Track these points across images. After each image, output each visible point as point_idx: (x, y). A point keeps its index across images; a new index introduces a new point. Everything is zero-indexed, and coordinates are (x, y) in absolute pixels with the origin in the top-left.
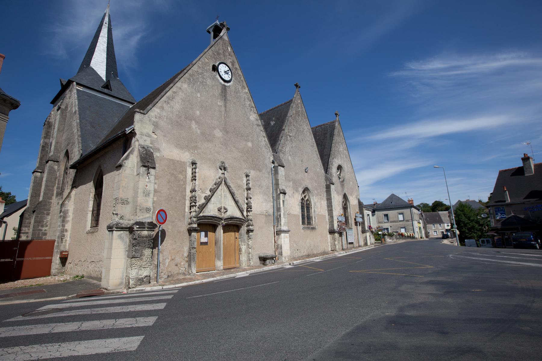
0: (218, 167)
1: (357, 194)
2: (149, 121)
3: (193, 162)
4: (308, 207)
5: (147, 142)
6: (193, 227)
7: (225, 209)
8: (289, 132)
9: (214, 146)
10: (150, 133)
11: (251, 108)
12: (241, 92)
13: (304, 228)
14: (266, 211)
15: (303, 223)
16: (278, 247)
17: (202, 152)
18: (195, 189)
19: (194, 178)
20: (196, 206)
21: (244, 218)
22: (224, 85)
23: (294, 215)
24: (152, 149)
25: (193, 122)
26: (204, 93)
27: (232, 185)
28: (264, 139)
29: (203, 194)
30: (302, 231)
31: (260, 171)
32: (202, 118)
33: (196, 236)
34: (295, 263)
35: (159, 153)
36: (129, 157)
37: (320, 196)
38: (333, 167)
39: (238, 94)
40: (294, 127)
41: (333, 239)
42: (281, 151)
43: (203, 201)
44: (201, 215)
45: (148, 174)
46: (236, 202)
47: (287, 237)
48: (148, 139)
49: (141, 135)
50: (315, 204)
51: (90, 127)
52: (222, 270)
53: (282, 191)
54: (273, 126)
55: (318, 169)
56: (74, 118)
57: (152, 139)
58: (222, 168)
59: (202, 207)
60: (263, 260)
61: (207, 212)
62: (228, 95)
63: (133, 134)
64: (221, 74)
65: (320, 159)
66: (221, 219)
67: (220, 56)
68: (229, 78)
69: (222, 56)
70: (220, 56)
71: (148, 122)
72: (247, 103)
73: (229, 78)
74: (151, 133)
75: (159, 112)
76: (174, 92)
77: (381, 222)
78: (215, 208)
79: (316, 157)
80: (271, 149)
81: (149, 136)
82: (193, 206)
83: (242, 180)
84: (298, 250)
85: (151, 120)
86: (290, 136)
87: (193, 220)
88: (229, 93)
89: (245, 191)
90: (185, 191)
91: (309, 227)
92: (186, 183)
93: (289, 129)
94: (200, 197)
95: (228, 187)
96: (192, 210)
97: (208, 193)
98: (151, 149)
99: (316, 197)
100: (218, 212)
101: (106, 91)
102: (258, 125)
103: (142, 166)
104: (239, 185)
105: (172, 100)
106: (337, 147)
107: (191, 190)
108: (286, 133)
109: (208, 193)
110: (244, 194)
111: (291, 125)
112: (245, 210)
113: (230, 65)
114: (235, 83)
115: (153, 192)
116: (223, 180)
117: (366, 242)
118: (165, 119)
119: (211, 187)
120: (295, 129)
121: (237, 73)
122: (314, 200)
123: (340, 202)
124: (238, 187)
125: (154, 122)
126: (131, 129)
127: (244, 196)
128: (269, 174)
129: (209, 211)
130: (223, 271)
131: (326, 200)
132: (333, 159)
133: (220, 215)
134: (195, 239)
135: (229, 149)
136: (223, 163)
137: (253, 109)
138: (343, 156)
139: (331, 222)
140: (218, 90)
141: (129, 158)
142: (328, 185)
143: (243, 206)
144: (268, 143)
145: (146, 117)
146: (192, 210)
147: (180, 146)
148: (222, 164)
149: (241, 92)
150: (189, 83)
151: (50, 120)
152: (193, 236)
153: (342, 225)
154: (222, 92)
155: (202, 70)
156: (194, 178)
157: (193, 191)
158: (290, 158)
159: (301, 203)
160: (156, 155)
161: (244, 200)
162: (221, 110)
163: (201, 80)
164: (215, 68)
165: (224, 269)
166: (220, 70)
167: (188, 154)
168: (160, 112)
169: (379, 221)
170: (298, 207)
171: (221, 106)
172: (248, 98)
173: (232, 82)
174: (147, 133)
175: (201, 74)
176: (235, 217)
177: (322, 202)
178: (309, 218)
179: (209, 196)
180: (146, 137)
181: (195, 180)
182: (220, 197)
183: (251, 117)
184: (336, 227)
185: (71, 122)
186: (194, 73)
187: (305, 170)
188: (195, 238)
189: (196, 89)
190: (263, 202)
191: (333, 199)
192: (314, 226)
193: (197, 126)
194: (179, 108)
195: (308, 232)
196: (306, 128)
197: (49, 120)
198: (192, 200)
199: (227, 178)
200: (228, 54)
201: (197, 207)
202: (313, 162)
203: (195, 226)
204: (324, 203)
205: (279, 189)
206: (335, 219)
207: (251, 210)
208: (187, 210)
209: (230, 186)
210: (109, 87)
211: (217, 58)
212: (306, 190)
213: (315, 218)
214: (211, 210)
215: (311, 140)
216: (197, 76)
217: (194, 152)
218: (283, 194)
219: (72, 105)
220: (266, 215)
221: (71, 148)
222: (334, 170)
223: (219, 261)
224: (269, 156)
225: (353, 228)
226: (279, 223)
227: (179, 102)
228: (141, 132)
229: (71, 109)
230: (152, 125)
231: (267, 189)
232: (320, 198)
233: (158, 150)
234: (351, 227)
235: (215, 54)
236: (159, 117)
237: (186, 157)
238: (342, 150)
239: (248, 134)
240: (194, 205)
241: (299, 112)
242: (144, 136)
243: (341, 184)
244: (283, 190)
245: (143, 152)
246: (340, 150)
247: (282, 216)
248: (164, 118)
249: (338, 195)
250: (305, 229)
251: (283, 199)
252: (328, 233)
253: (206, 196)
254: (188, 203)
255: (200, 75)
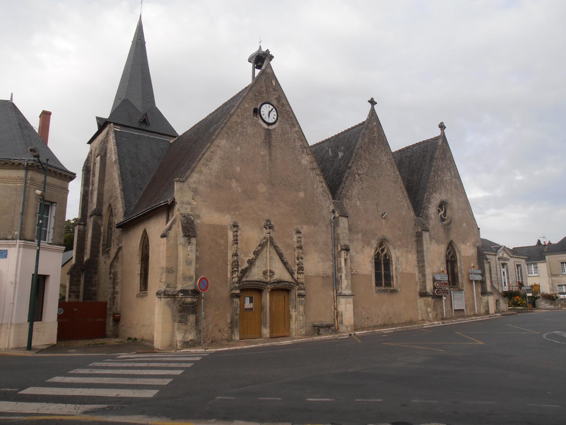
0: (263, 226)
1: (476, 240)
2: (189, 189)
3: (235, 224)
4: (388, 263)
5: (187, 210)
6: (236, 293)
7: (271, 272)
8: (357, 169)
9: (258, 203)
10: (189, 201)
11: (303, 149)
12: (289, 132)
13: (378, 292)
14: (323, 272)
15: (378, 284)
16: (337, 314)
17: (244, 212)
18: (237, 253)
19: (236, 241)
20: (238, 271)
21: (294, 282)
22: (268, 129)
23: (363, 275)
24: (192, 216)
25: (234, 181)
26: (245, 145)
27: (279, 245)
28: (320, 185)
29: (246, 258)
30: (376, 295)
31: (315, 224)
32: (242, 175)
33: (239, 302)
34: (358, 334)
35: (200, 219)
36: (172, 227)
37: (405, 249)
38: (429, 206)
39: (286, 136)
40: (366, 161)
41: (424, 305)
42: (345, 196)
43: (246, 265)
44: (244, 279)
45: (189, 243)
46: (285, 264)
47: (349, 303)
48: (189, 207)
49: (182, 204)
50: (397, 259)
51: (130, 177)
52: (268, 338)
53: (344, 248)
54: (341, 160)
55: (404, 212)
56: (115, 168)
57: (192, 206)
58: (267, 227)
59: (244, 272)
60: (317, 329)
61: (251, 277)
62: (273, 141)
63: (173, 203)
64: (264, 118)
65: (407, 198)
66: (267, 283)
67: (262, 96)
68: (274, 119)
69: (265, 94)
70: (262, 96)
71: (187, 190)
72: (297, 144)
73: (274, 119)
74: (190, 200)
75: (197, 176)
76: (212, 152)
77: (557, 275)
78: (260, 272)
79: (401, 196)
80: (330, 196)
81: (189, 203)
82: (235, 271)
83: (292, 238)
84: (368, 318)
85: (190, 187)
86: (359, 175)
87: (236, 286)
88: (275, 138)
89: (295, 251)
90: (227, 256)
91: (387, 290)
92: (228, 247)
93: (357, 165)
94: (243, 261)
95: (276, 247)
96: (234, 276)
97: (252, 256)
98: (192, 217)
99: (399, 250)
100: (263, 276)
101: (144, 127)
102: (313, 169)
103: (184, 236)
104: (288, 244)
105: (209, 161)
106: (440, 176)
107: (233, 254)
108: (353, 171)
109: (252, 256)
110: (295, 254)
111: (362, 159)
112: (296, 273)
113: (275, 103)
114: (281, 123)
115: (194, 260)
116: (269, 240)
117: (487, 309)
118: (204, 183)
119: (254, 249)
120: (367, 163)
121: (285, 110)
122: (396, 254)
123: (441, 253)
124: (287, 246)
125: (193, 188)
126: (172, 199)
127: (295, 256)
128: (327, 228)
129: (254, 276)
130: (270, 339)
131: (416, 252)
132: (431, 194)
133: (265, 279)
134: (238, 305)
135: (275, 204)
136: (268, 221)
137: (307, 150)
138: (451, 187)
139: (422, 282)
140: (261, 138)
141: (172, 228)
142: (420, 231)
143: (293, 268)
144: (326, 188)
145: (185, 185)
146: (234, 276)
147: (219, 209)
148: (267, 222)
149: (289, 132)
150: (228, 137)
151: (89, 164)
152: (236, 302)
153: (442, 286)
154: (266, 139)
155: (242, 119)
156: (236, 241)
157: (236, 255)
158: (358, 203)
159: (374, 260)
160: (198, 221)
161: (295, 261)
162: (265, 160)
163: (241, 131)
164: (257, 112)
165: (270, 337)
166: (262, 113)
167: (229, 216)
168: (199, 177)
169: (552, 274)
170: (370, 264)
171: (265, 155)
172: (299, 137)
173: (277, 123)
174: (187, 201)
175: (240, 124)
176: (283, 281)
177: (410, 256)
178: (388, 277)
179: (253, 259)
180: (186, 205)
181: (237, 243)
182: (265, 259)
183: (303, 160)
184: (429, 287)
185: (111, 172)
186: (232, 125)
187: (382, 216)
188: (238, 304)
189: (235, 142)
190: (319, 262)
191: (427, 251)
192: (395, 287)
193: (237, 185)
194: (218, 168)
195: (385, 296)
196: (385, 158)
197: (88, 164)
198: (234, 266)
199: (274, 238)
200: (272, 90)
201: (239, 272)
202: (395, 204)
203: (238, 291)
204: (413, 257)
205: (340, 246)
206: (429, 279)
207: (302, 272)
208: (229, 275)
209: (277, 246)
210: (146, 121)
211: (258, 98)
212: (382, 243)
213: (397, 277)
214: (255, 275)
215: (392, 174)
216: (237, 127)
217: (235, 214)
218: (345, 251)
219: (111, 151)
220: (323, 277)
221: (114, 202)
222: (432, 210)
223: (265, 329)
224: (327, 205)
225: (464, 289)
226: (340, 286)
227: (218, 162)
228: (182, 201)
229: (110, 155)
230: (192, 192)
231: (325, 246)
232: (407, 251)
233: (199, 217)
234: (462, 288)
235: (257, 94)
236: (198, 182)
237: (226, 220)
238: (448, 178)
239: (299, 182)
240: (237, 271)
241: (374, 139)
242: (184, 204)
243: (444, 229)
244: (345, 245)
245: (184, 221)
246: (445, 179)
247: (343, 277)
248: (203, 183)
249: (439, 245)
250: (381, 292)
251: (346, 258)
252: (418, 297)
253: (249, 260)
254: (229, 267)
255: (239, 125)
